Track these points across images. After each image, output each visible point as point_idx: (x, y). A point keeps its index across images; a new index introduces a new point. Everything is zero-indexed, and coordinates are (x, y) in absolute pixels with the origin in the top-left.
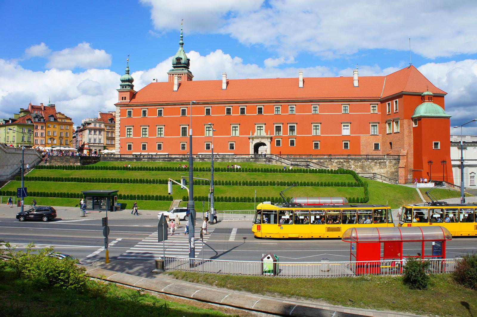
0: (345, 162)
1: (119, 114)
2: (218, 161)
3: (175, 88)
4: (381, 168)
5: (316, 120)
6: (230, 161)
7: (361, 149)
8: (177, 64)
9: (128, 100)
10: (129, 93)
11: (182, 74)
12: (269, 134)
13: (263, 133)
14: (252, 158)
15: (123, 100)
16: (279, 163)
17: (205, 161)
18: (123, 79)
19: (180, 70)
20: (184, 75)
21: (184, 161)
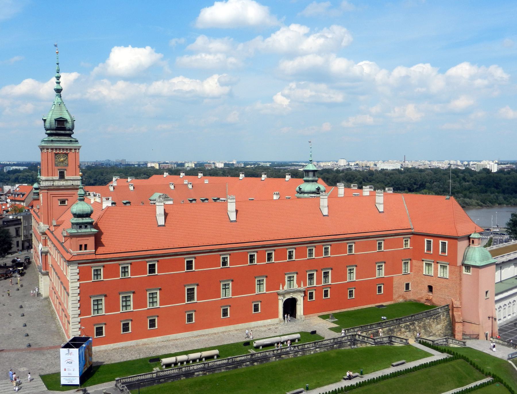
0: (411, 324)
1: (78, 277)
2: (299, 355)
3: (161, 221)
4: (438, 324)
5: (351, 262)
6: (312, 352)
7: (394, 291)
8: (57, 129)
9: (91, 250)
10: (92, 239)
11: (71, 149)
12: (302, 285)
13: (296, 286)
14: (336, 343)
15: (81, 249)
16: (364, 345)
17: (283, 358)
18: (81, 213)
19: (66, 141)
20: (73, 151)
21: (255, 364)
